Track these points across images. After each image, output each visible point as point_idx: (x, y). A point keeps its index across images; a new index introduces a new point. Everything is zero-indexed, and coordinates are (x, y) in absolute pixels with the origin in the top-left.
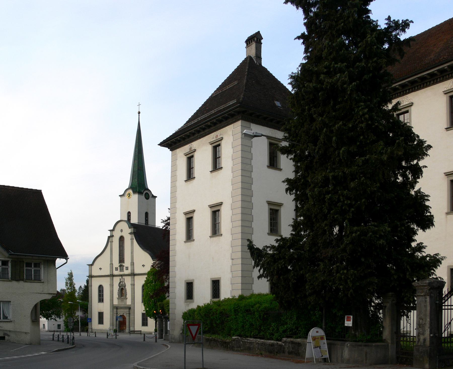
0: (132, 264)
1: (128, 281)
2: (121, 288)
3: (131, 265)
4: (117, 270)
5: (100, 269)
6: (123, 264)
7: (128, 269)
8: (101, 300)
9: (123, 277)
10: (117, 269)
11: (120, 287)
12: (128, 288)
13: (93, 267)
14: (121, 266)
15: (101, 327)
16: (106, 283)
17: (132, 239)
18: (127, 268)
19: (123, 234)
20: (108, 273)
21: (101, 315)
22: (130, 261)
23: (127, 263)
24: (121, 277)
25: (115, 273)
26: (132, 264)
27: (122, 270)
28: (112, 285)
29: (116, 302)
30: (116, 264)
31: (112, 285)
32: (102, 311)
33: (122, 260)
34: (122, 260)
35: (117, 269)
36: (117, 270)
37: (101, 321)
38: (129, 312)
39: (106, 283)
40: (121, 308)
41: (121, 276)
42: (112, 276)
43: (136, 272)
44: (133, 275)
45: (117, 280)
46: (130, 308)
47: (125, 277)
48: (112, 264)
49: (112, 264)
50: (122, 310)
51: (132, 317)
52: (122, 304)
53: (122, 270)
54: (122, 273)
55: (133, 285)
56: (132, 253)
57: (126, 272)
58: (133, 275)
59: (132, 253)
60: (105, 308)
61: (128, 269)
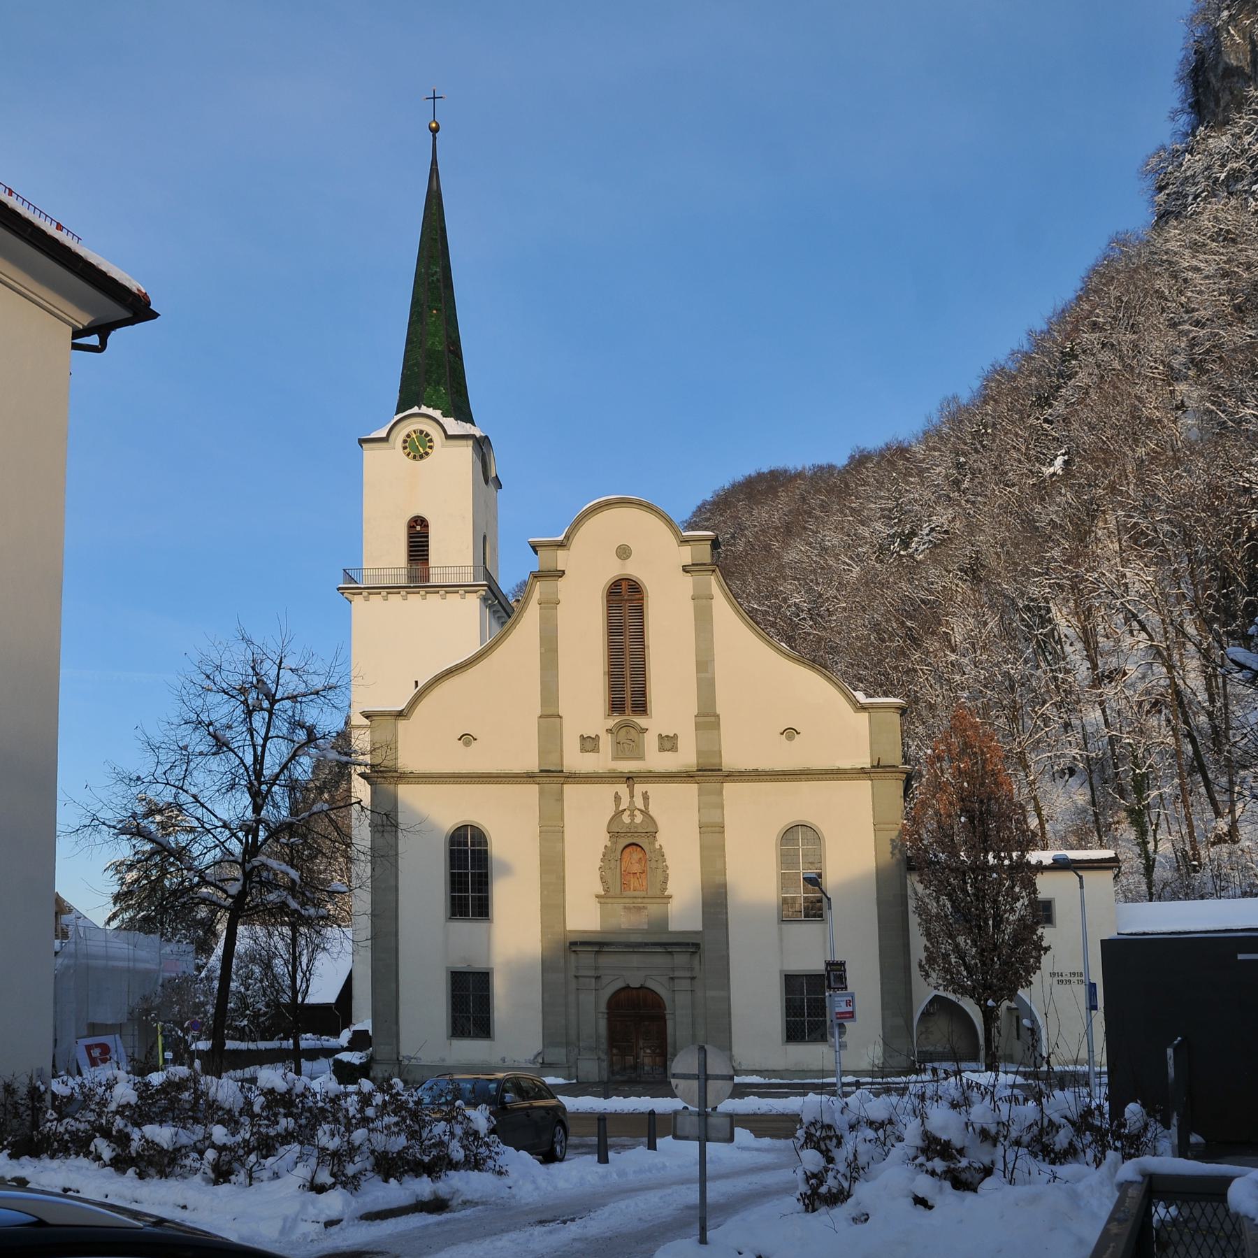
0: (708, 720)
2: (623, 842)
3: (698, 726)
4: (595, 749)
5: (467, 739)
6: (641, 721)
7: (674, 748)
9: (639, 788)
10: (589, 744)
11: (614, 835)
13: (402, 724)
17: (702, 600)
19: (632, 569)
20: (531, 763)
22: (692, 707)
24: (622, 789)
25: (574, 760)
26: (708, 720)
29: (584, 916)
32: (479, 966)
33: (628, 693)
34: (628, 693)
36: (595, 749)
38: (692, 969)
41: (630, 779)
42: (551, 777)
43: (731, 760)
44: (709, 773)
46: (689, 946)
47: (653, 789)
48: (550, 717)
49: (550, 717)
50: (635, 960)
56: (704, 664)
57: (656, 760)
59: (704, 664)
61: (674, 748)
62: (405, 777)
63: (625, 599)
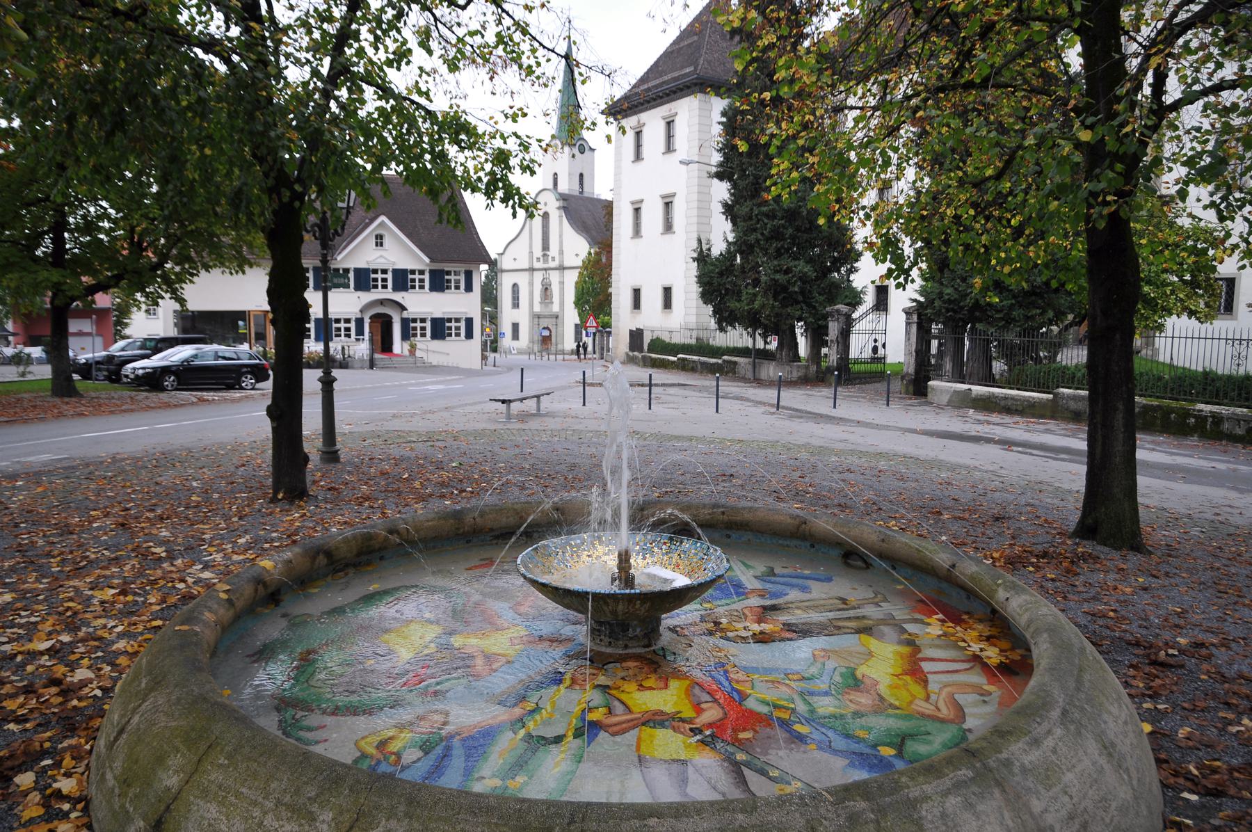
0: (561, 252)
1: (554, 277)
8: (516, 305)
10: (538, 259)
12: (555, 288)
14: (544, 255)
15: (515, 344)
16: (522, 280)
17: (560, 217)
18: (553, 259)
21: (515, 327)
23: (554, 251)
25: (537, 265)
26: (561, 252)
27: (546, 261)
28: (531, 284)
29: (537, 308)
30: (538, 252)
31: (531, 284)
33: (546, 247)
34: (546, 247)
35: (538, 259)
37: (515, 335)
39: (522, 280)
40: (545, 317)
41: (545, 269)
42: (532, 270)
43: (566, 264)
44: (562, 268)
45: (538, 277)
48: (531, 252)
49: (531, 252)
51: (560, 329)
52: (546, 312)
53: (546, 261)
54: (546, 266)
55: (562, 283)
56: (561, 236)
57: (552, 264)
58: (562, 268)
59: (561, 236)
60: (522, 316)
62: (502, 271)
63: (546, 216)
